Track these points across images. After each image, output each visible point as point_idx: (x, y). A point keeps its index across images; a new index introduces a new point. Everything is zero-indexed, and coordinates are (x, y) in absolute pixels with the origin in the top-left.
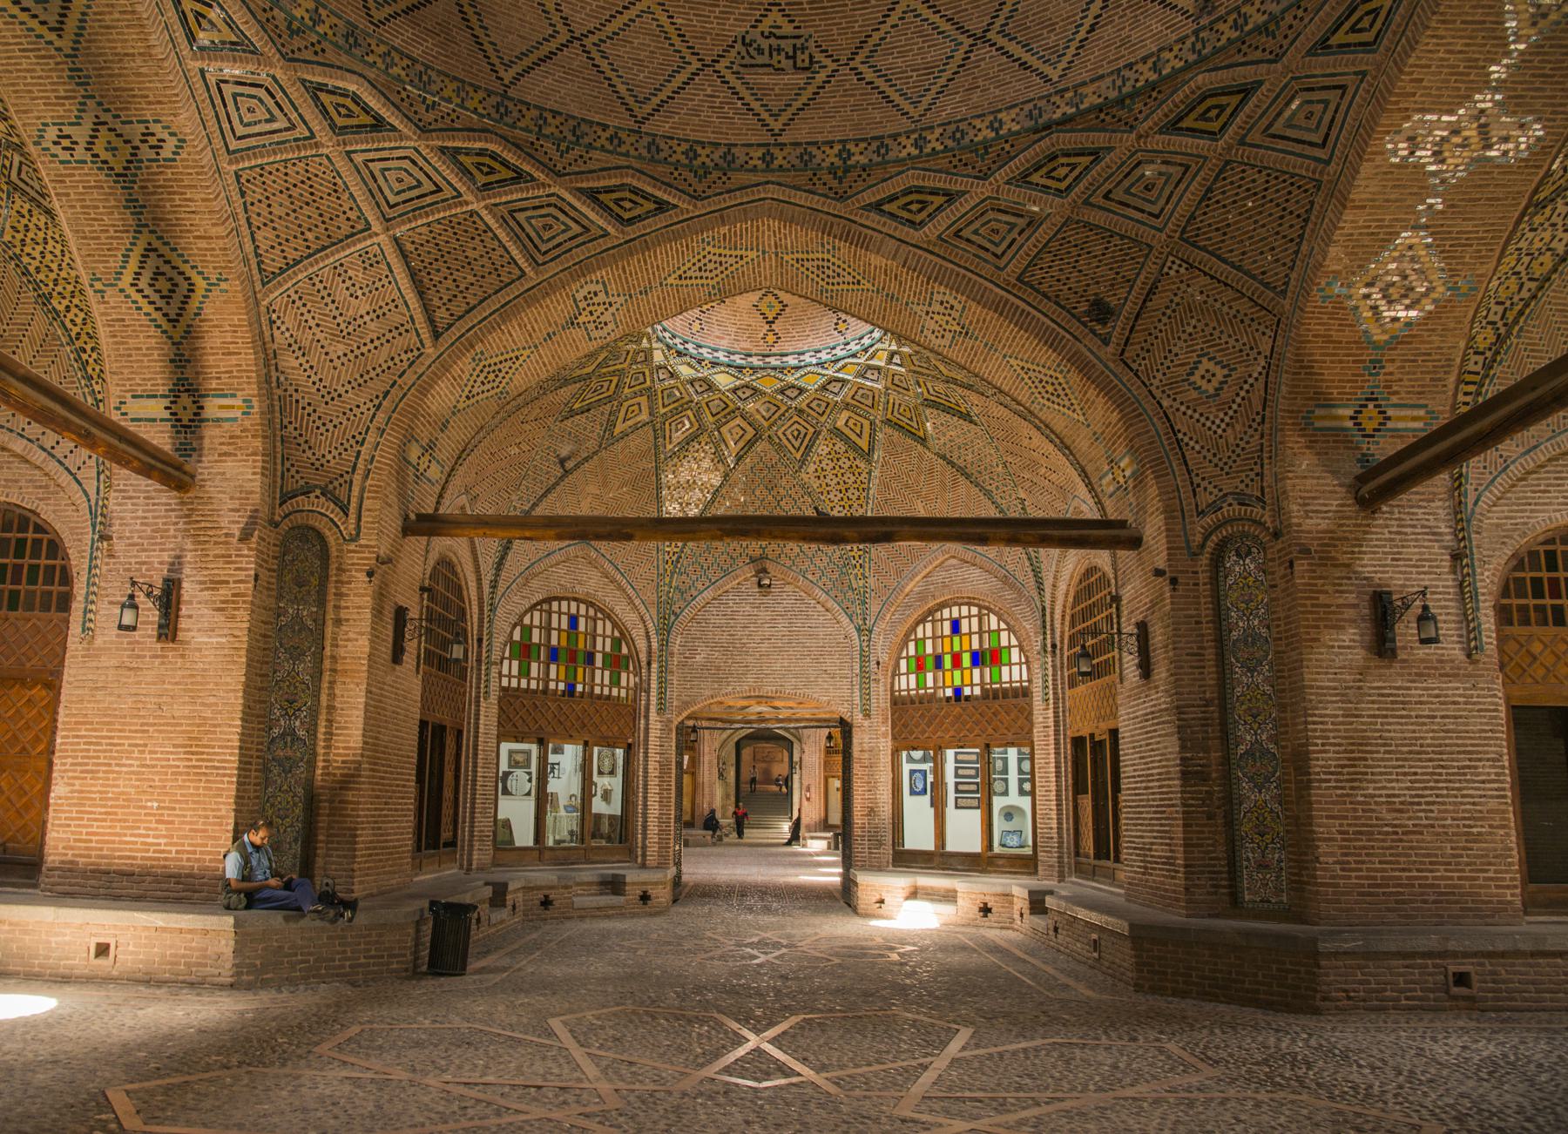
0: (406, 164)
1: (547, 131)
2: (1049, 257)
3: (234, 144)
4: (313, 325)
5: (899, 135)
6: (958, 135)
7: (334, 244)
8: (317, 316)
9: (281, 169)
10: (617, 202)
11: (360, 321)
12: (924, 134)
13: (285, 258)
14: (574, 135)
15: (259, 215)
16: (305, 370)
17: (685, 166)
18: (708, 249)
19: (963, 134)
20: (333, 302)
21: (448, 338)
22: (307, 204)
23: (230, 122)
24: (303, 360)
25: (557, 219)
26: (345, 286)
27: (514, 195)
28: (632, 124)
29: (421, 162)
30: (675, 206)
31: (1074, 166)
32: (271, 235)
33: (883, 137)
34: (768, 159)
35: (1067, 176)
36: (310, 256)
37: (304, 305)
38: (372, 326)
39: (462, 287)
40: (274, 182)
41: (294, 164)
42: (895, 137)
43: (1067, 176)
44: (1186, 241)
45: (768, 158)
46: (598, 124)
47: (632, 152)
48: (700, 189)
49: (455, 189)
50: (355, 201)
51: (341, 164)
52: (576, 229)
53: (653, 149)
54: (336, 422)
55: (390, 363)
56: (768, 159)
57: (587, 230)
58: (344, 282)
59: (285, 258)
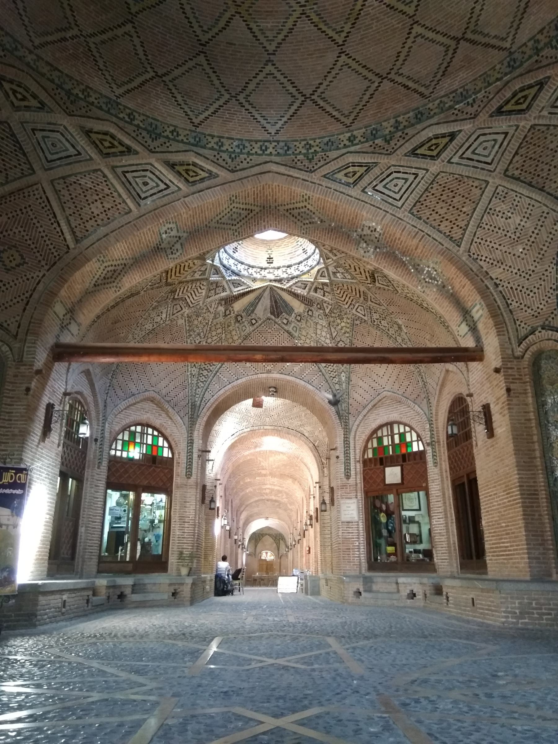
0: (482, 139)
3: (400, 204)
4: (498, 246)
7: (478, 203)
8: (496, 241)
9: (429, 194)
13: (461, 228)
15: (435, 220)
16: (508, 270)
20: (499, 229)
22: (454, 197)
23: (391, 197)
24: (502, 267)
26: (500, 217)
32: (447, 223)
36: (471, 217)
37: (486, 241)
40: (431, 202)
41: (432, 188)
51: (450, 169)
58: (498, 216)
59: (461, 228)
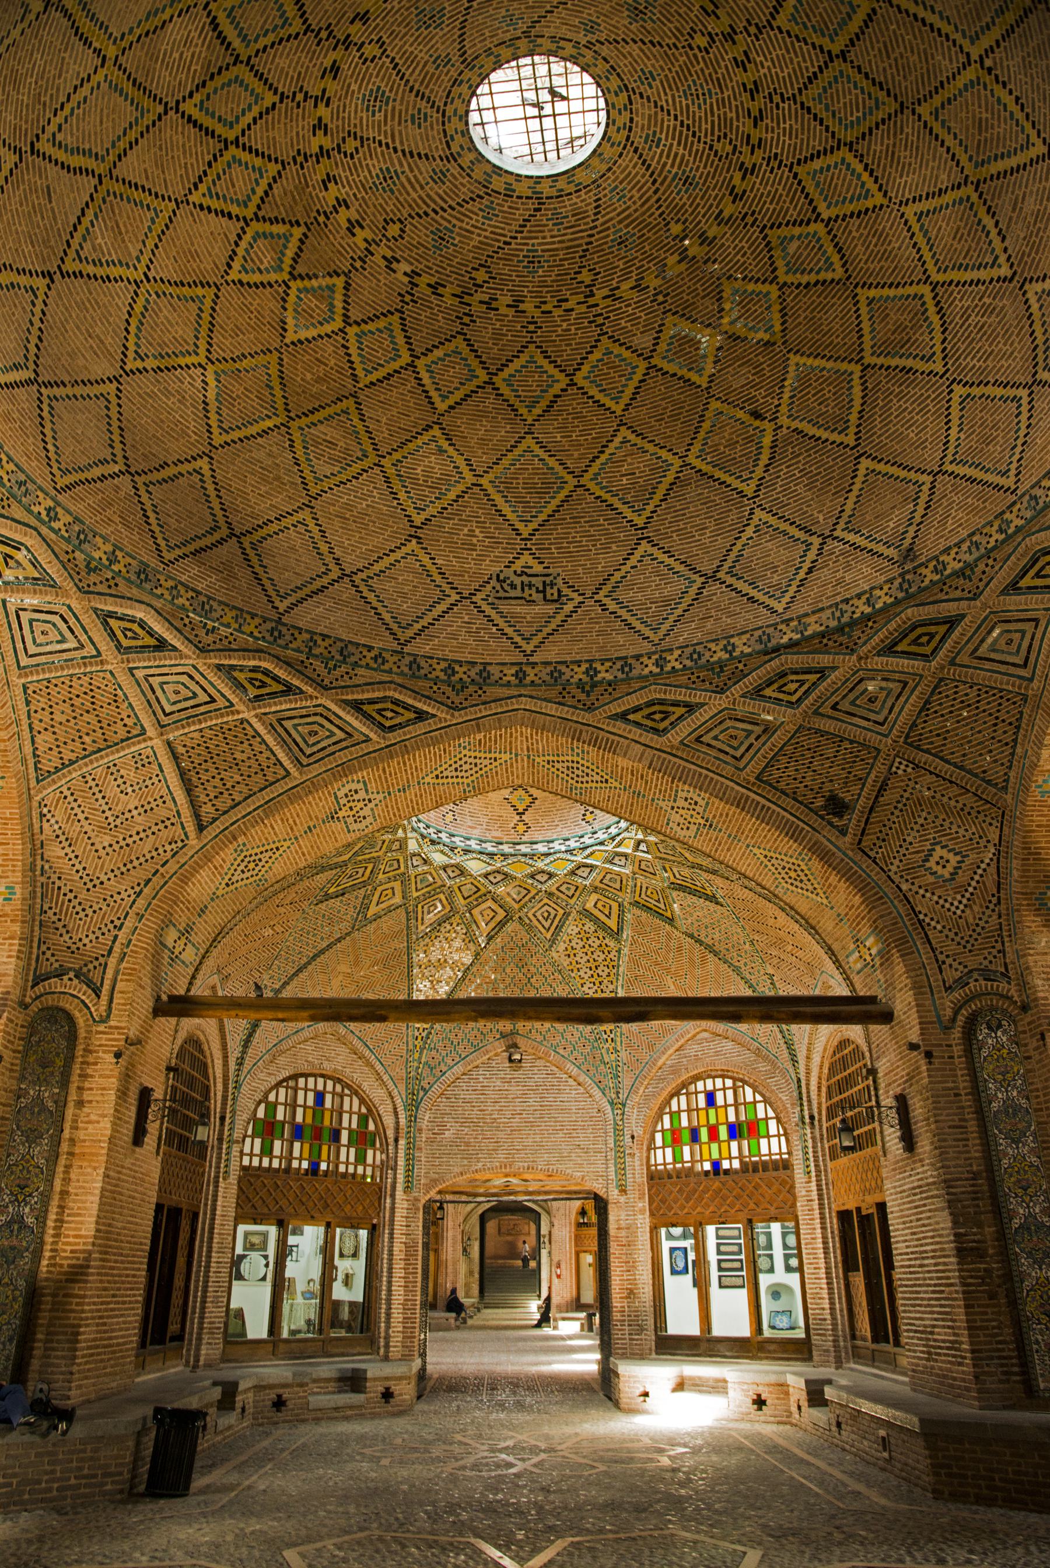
1: (316, 651)
2: (785, 759)
5: (641, 656)
6: (695, 656)
7: (109, 747)
10: (379, 712)
11: (128, 815)
12: (664, 655)
14: (341, 654)
17: (443, 681)
18: (464, 752)
19: (700, 655)
21: (211, 832)
25: (323, 726)
27: (283, 705)
28: (395, 645)
29: (198, 677)
30: (434, 716)
31: (802, 683)
33: (626, 658)
34: (520, 675)
35: (796, 691)
38: (139, 819)
39: (229, 785)
42: (637, 657)
43: (796, 691)
44: (911, 745)
45: (521, 675)
46: (364, 646)
47: (395, 669)
48: (457, 701)
49: (228, 700)
50: (133, 709)
52: (340, 735)
53: (414, 666)
54: (96, 907)
55: (154, 854)
56: (520, 675)
57: (350, 735)
